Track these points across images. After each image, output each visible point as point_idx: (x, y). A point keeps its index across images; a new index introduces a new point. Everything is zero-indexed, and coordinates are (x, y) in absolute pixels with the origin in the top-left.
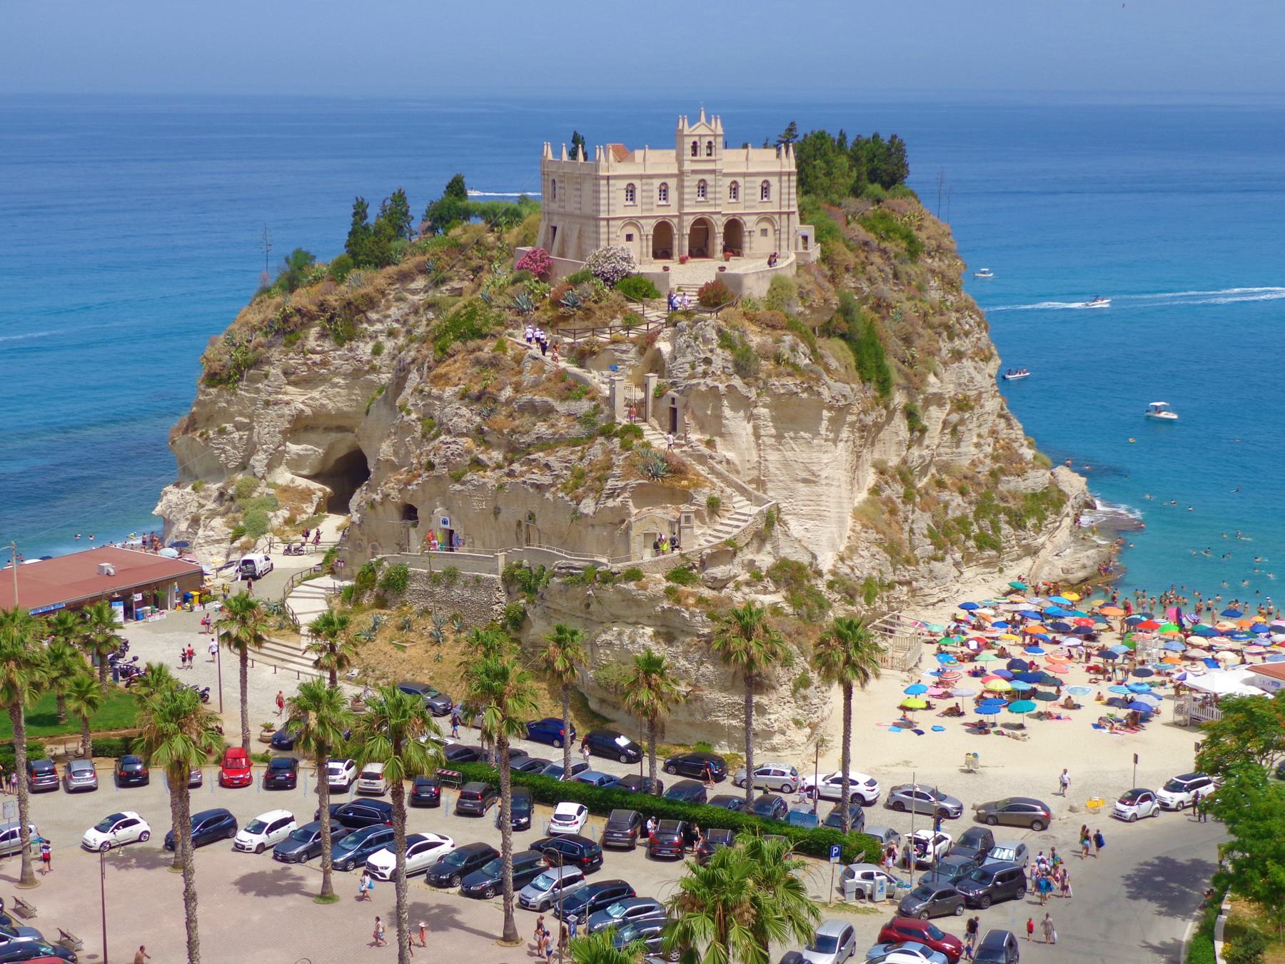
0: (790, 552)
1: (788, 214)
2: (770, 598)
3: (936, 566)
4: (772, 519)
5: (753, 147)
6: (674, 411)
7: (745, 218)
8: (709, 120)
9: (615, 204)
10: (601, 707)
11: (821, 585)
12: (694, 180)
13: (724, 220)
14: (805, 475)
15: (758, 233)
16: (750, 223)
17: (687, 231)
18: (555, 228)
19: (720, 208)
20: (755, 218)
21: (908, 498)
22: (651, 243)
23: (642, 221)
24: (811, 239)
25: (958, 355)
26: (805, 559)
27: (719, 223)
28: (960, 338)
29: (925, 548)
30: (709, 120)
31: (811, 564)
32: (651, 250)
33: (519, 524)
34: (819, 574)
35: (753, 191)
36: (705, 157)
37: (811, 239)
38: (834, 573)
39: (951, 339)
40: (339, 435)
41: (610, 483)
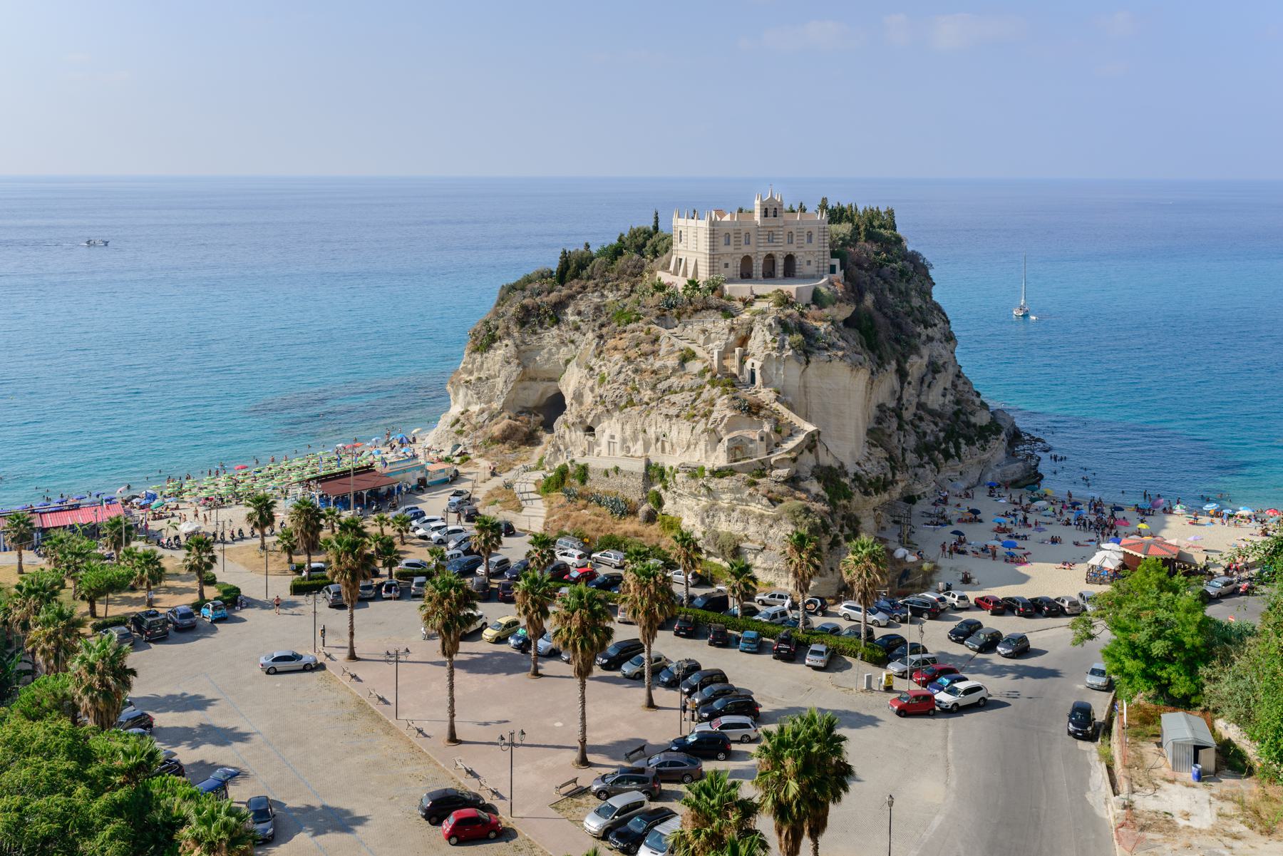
0: (826, 460)
3: (920, 471)
7: (797, 254)
10: (708, 557)
11: (846, 481)
17: (762, 262)
18: (681, 260)
21: (900, 428)
22: (739, 269)
24: (838, 268)
25: (930, 339)
26: (836, 465)
28: (931, 327)
29: (911, 458)
31: (839, 467)
32: (739, 273)
33: (657, 440)
34: (846, 474)
37: (838, 268)
38: (856, 474)
39: (926, 328)
40: (549, 384)
41: (715, 415)
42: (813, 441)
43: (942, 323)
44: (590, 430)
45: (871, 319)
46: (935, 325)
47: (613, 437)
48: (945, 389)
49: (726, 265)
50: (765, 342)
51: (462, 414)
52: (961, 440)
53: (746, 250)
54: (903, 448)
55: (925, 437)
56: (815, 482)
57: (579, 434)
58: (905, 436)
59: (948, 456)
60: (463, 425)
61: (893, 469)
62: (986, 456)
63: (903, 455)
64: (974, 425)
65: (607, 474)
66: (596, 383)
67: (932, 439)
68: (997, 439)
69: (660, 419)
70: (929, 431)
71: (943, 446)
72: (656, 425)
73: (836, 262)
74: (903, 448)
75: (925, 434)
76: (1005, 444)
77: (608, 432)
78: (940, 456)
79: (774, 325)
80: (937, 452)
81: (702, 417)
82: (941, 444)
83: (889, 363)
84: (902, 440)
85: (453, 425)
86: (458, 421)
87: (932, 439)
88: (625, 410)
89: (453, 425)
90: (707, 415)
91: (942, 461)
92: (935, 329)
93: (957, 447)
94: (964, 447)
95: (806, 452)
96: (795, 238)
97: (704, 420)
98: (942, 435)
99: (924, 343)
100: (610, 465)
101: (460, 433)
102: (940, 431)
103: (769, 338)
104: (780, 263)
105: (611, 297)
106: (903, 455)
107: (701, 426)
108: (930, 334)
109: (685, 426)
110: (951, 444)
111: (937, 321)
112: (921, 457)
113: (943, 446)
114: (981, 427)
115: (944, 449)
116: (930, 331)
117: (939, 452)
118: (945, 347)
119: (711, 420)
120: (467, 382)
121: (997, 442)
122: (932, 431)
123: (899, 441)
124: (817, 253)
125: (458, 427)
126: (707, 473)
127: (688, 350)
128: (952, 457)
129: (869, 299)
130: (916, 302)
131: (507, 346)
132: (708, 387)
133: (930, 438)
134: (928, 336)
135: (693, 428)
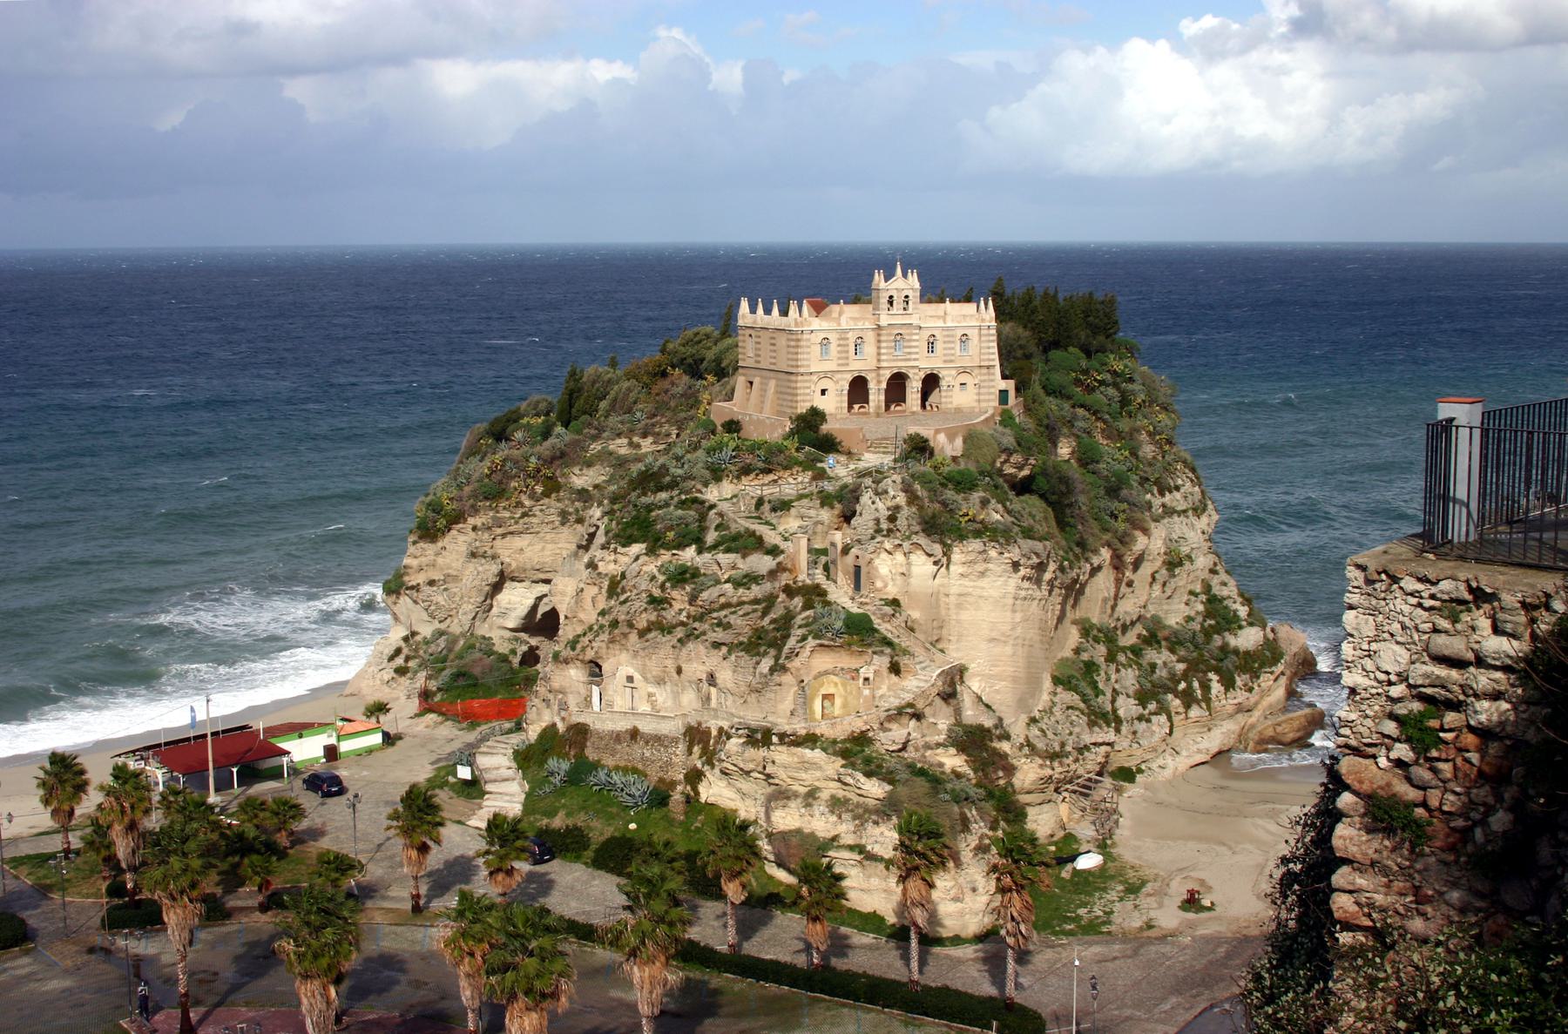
0: (971, 715)
1: (988, 367)
2: (952, 761)
3: (1141, 727)
4: (954, 679)
5: (952, 301)
6: (858, 569)
8: (905, 275)
9: (813, 360)
11: (1005, 747)
12: (890, 335)
13: (922, 375)
14: (994, 634)
15: (958, 386)
16: (947, 378)
17: (884, 385)
18: (751, 383)
19: (917, 365)
20: (954, 372)
21: (1111, 658)
22: (846, 398)
23: (839, 376)
24: (1012, 394)
25: (1169, 512)
27: (917, 377)
28: (1170, 492)
29: (1127, 707)
30: (905, 275)
31: (996, 727)
34: (1007, 737)
35: (952, 345)
36: (902, 312)
39: (1162, 494)
42: (952, 684)
43: (1189, 484)
44: (595, 670)
45: (1065, 480)
46: (1177, 488)
47: (630, 679)
48: (1191, 593)
49: (823, 392)
50: (877, 521)
51: (406, 639)
52: (1212, 676)
53: (857, 366)
54: (1114, 690)
55: (1153, 672)
56: (953, 751)
57: (575, 675)
58: (1118, 671)
59: (1188, 699)
60: (407, 659)
61: (1092, 724)
62: (1253, 698)
63: (1113, 701)
64: (1236, 652)
65: (617, 737)
66: (604, 591)
67: (1164, 673)
68: (1272, 673)
69: (701, 648)
70: (1159, 662)
71: (1182, 685)
72: (698, 661)
73: (1009, 385)
74: (1114, 690)
75: (1153, 666)
76: (1283, 681)
77: (627, 670)
78: (1177, 702)
79: (892, 493)
80: (1170, 696)
81: (770, 646)
82: (1179, 682)
83: (1096, 552)
84: (1113, 677)
85: (391, 659)
86: (398, 651)
87: (1164, 673)
88: (651, 636)
89: (391, 659)
90: (777, 644)
91: (1181, 710)
92: (1177, 495)
93: (1206, 687)
94: (1216, 687)
95: (938, 701)
96: (939, 346)
97: (773, 652)
98: (1181, 667)
99: (1156, 520)
100: (623, 725)
101: (401, 671)
102: (1178, 661)
103: (884, 513)
104: (914, 388)
105: (647, 445)
106: (1113, 701)
107: (766, 664)
108: (1169, 504)
109: (746, 660)
110: (1196, 684)
111: (1180, 482)
112: (1143, 704)
113: (1182, 685)
114: (1247, 653)
115: (1184, 690)
116: (1168, 498)
117: (1176, 696)
118: (1193, 525)
119: (786, 650)
120: (412, 588)
121: (1272, 677)
122: (1165, 664)
123: (1108, 679)
124: (976, 371)
125: (400, 661)
126: (775, 739)
127: (752, 534)
128: (1198, 702)
129: (1064, 450)
130: (1148, 450)
131: (474, 528)
132: (782, 596)
133: (1161, 673)
134: (1164, 505)
135: (758, 663)
